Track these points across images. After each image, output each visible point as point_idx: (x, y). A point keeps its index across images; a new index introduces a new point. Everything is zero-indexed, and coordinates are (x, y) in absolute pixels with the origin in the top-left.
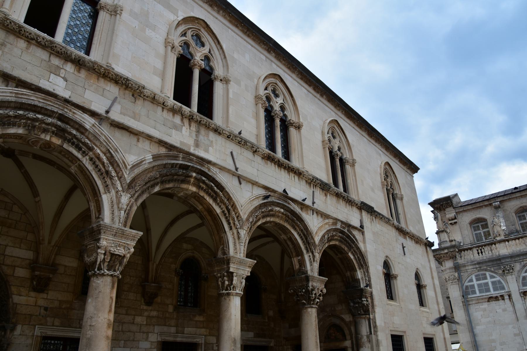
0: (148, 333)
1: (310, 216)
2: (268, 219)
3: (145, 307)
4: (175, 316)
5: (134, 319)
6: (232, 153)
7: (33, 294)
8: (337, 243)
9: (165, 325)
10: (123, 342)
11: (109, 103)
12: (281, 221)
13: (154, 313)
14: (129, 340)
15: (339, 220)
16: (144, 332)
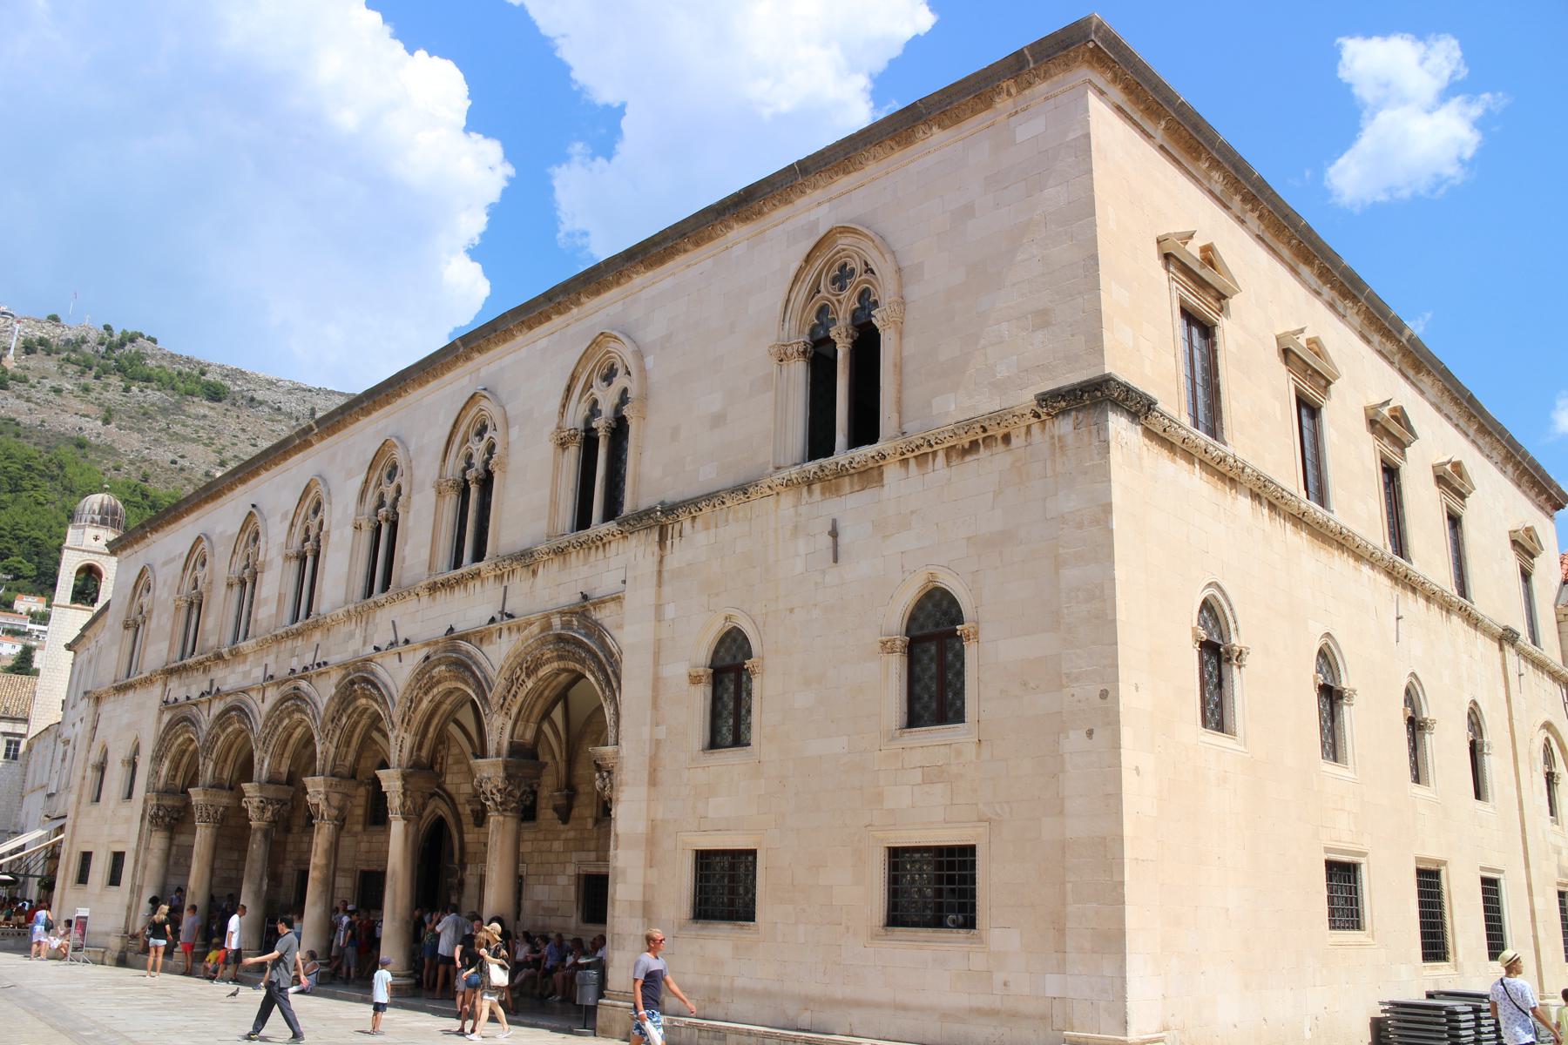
0: (564, 863)
1: (496, 644)
2: (435, 691)
3: (562, 827)
4: (595, 835)
5: (551, 846)
6: (393, 622)
7: (476, 829)
8: (555, 665)
9: (584, 851)
10: (542, 877)
11: (314, 653)
12: (453, 683)
13: (572, 834)
14: (548, 875)
15: (553, 614)
16: (561, 863)
